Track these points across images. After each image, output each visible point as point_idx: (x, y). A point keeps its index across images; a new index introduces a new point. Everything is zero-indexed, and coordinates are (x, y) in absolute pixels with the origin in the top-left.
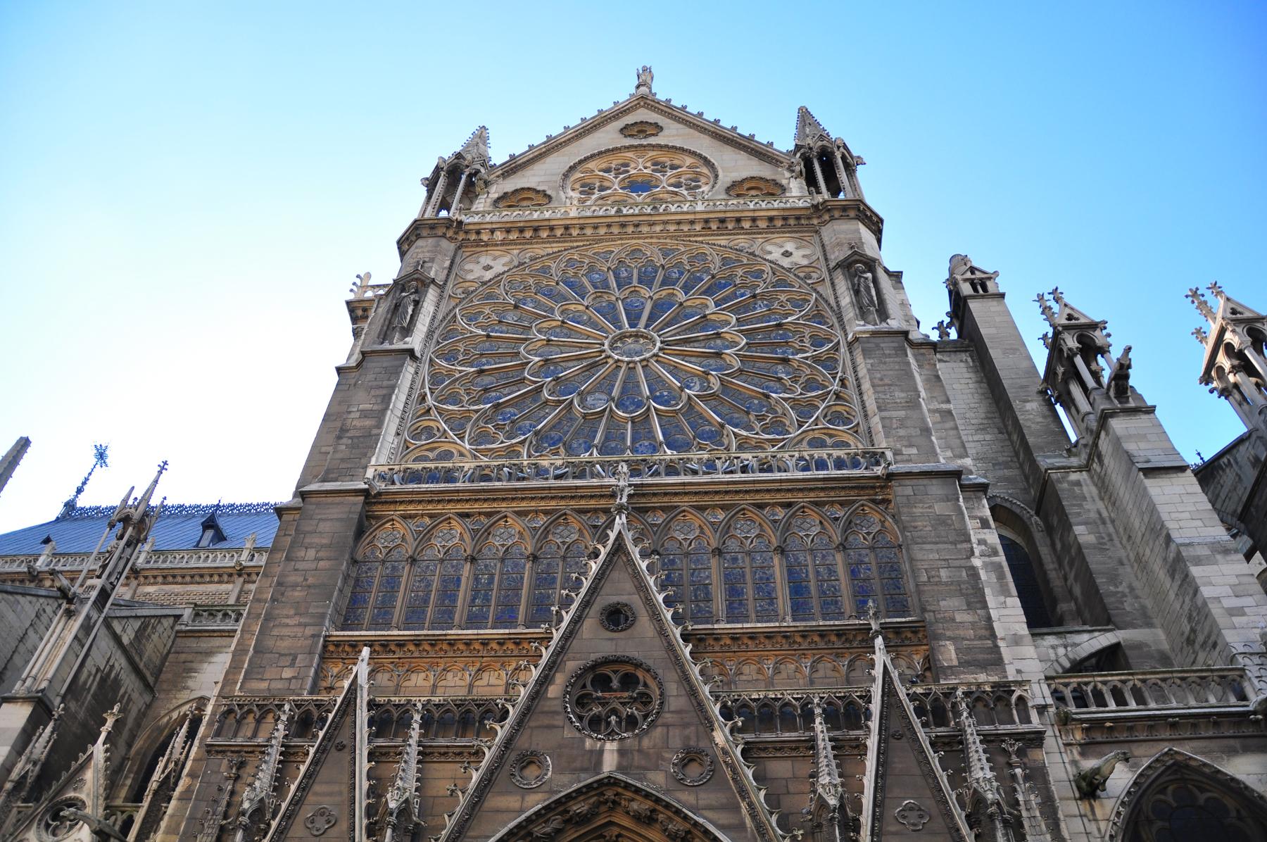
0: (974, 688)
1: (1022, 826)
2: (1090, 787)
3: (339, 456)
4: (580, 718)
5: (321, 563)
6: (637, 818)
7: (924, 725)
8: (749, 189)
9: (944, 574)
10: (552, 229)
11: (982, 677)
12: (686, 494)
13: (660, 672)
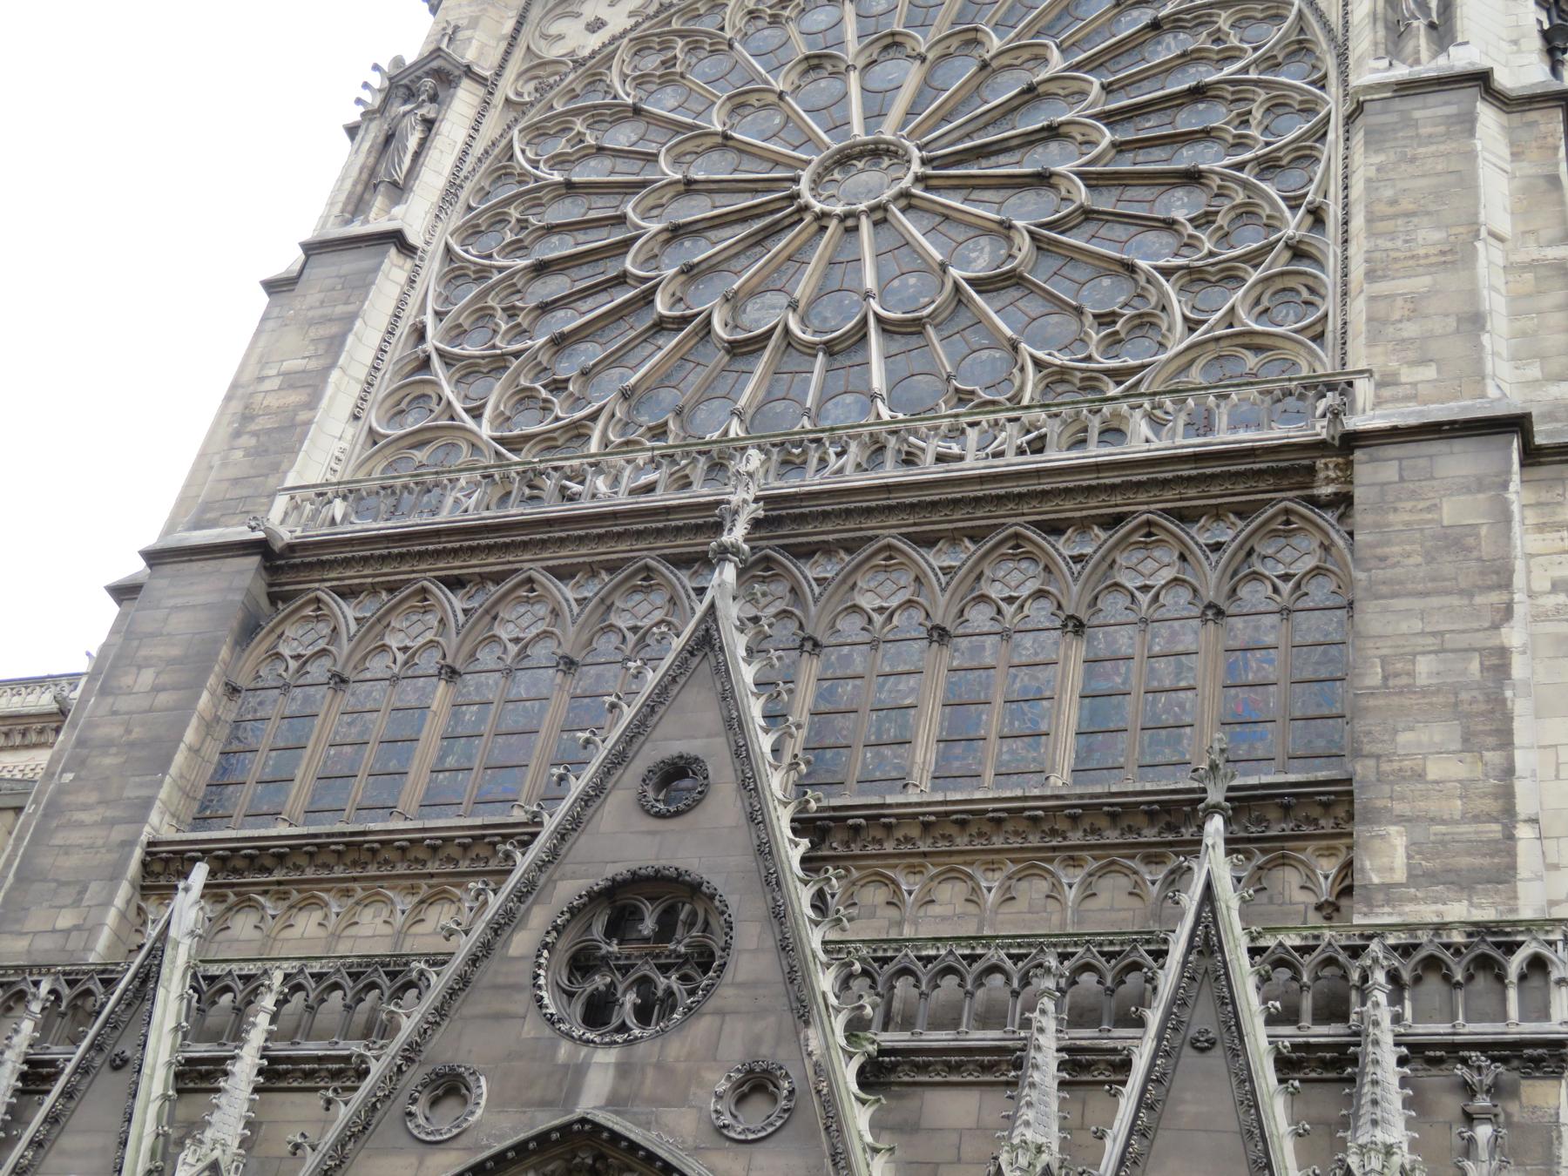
0: (1423, 937)
3: (232, 472)
5: (163, 698)
12: (890, 509)
13: (732, 900)
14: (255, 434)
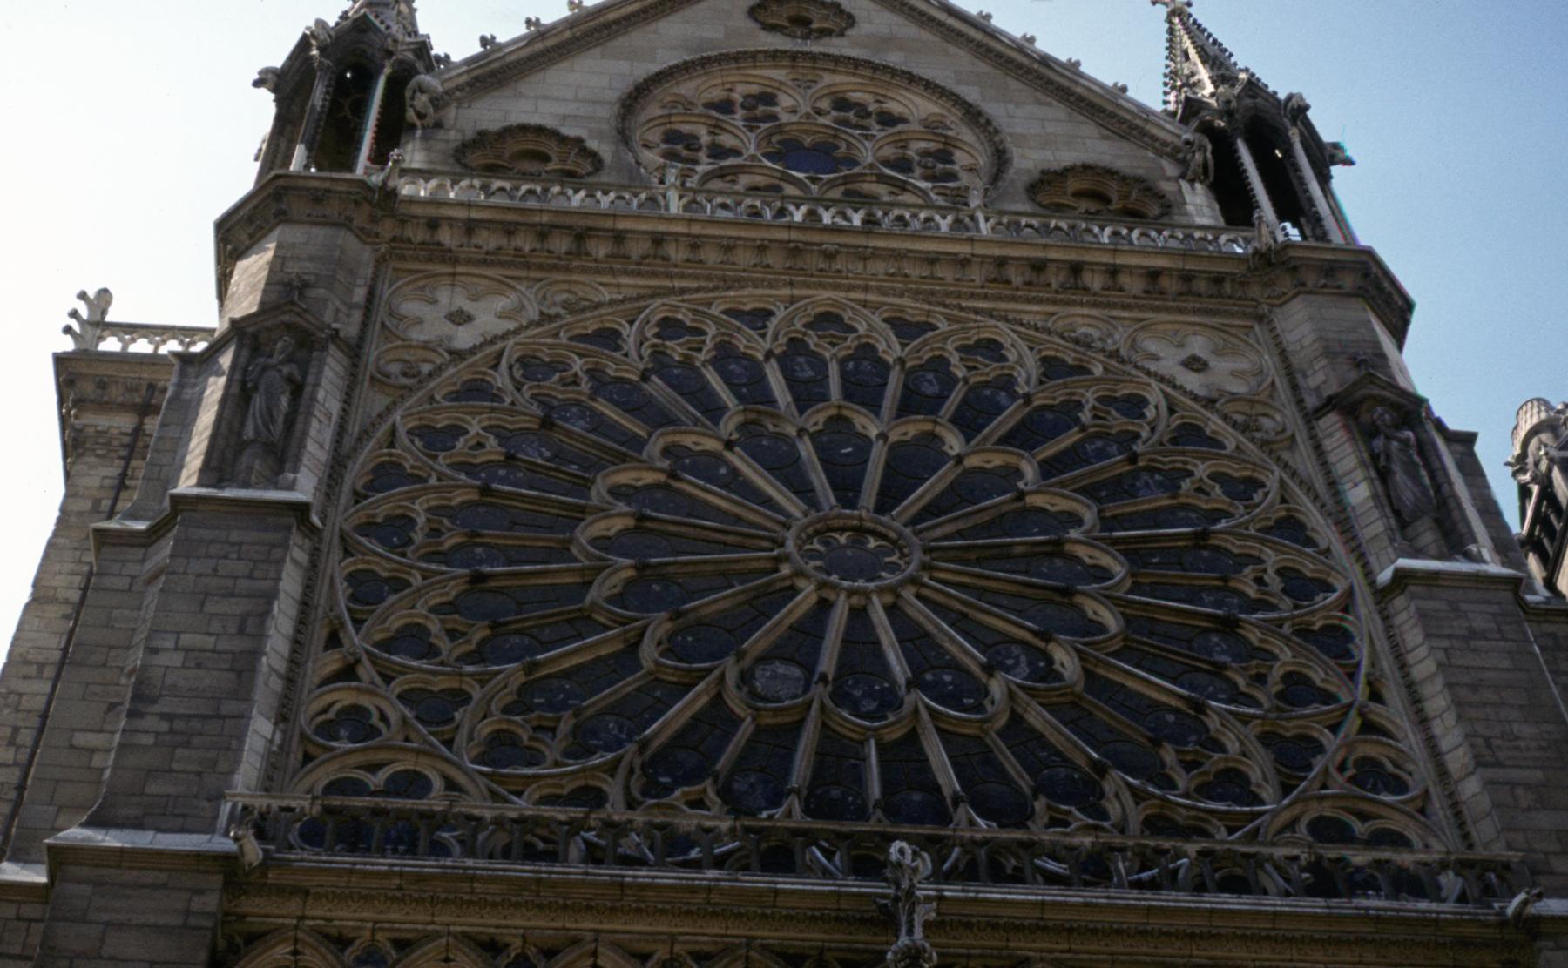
8: (1078, 195)
10: (619, 237)
14: (164, 716)
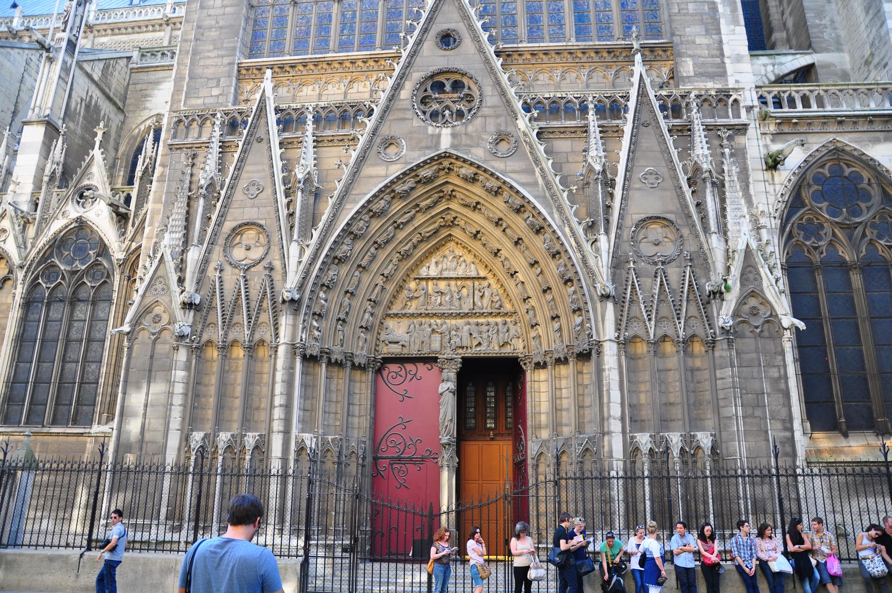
0: (703, 92)
1: (724, 186)
2: (774, 163)
4: (424, 113)
5: (228, 10)
6: (465, 179)
7: (665, 117)
9: (691, 7)
11: (710, 85)
13: (479, 79)
